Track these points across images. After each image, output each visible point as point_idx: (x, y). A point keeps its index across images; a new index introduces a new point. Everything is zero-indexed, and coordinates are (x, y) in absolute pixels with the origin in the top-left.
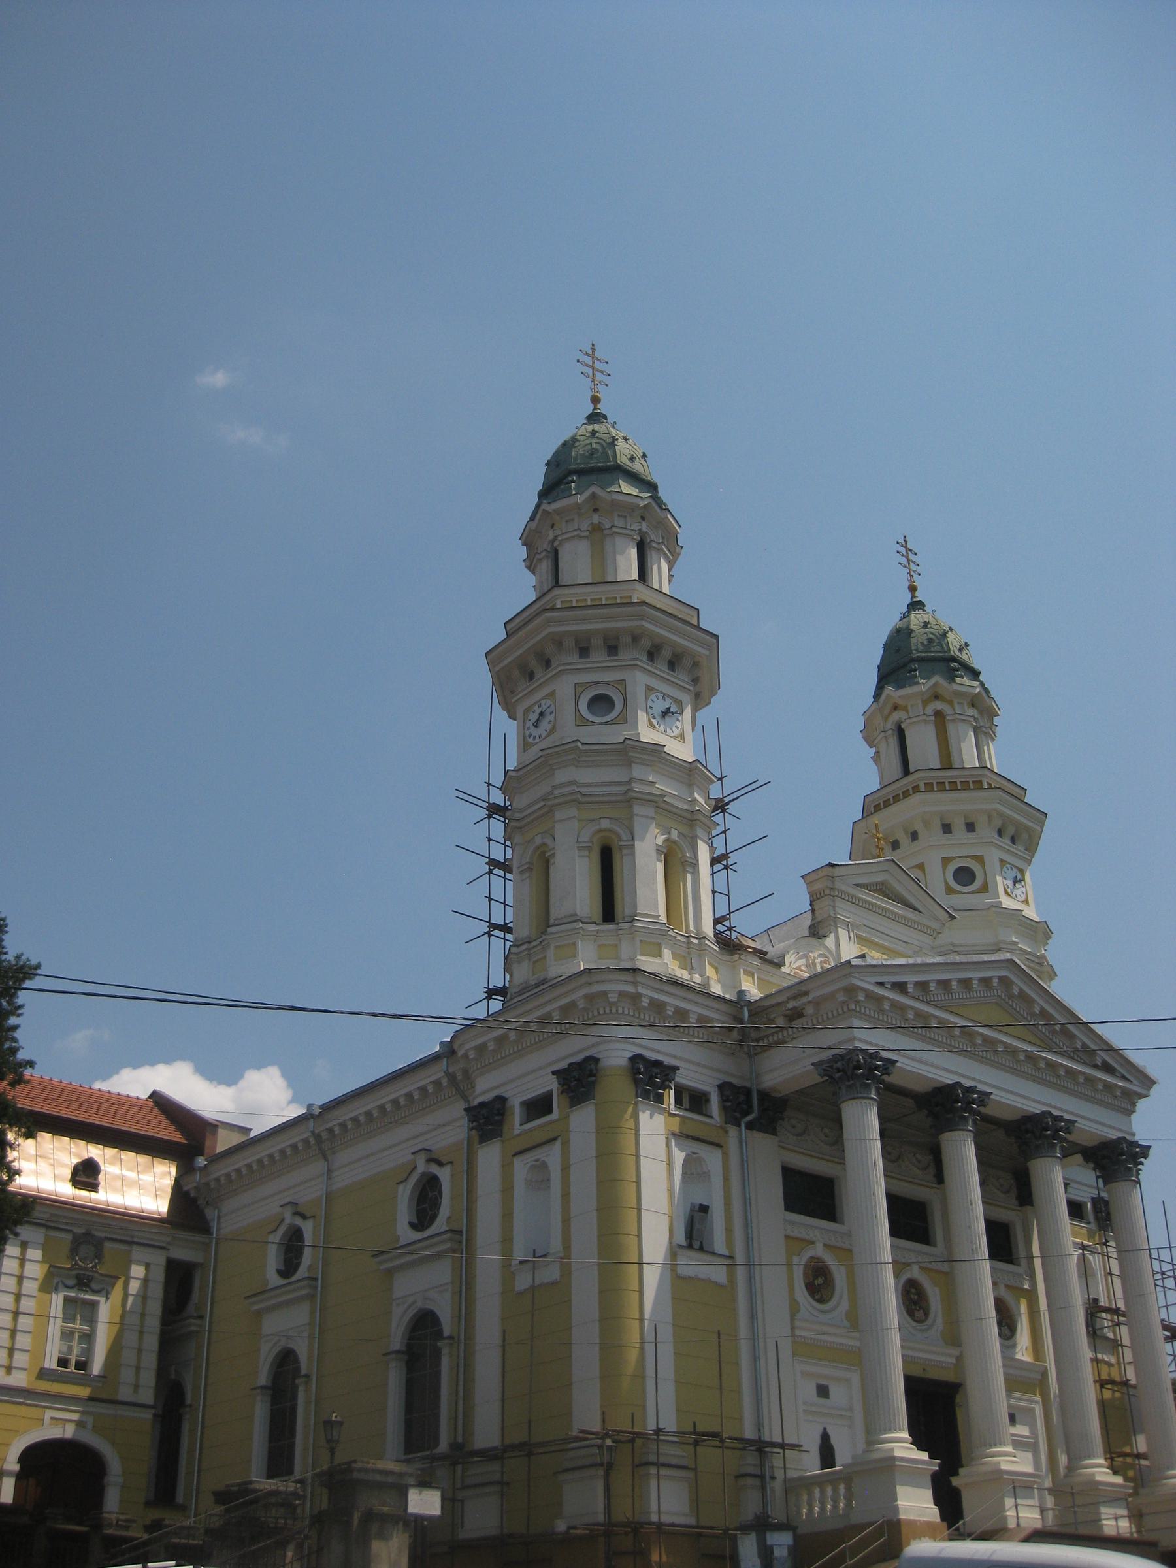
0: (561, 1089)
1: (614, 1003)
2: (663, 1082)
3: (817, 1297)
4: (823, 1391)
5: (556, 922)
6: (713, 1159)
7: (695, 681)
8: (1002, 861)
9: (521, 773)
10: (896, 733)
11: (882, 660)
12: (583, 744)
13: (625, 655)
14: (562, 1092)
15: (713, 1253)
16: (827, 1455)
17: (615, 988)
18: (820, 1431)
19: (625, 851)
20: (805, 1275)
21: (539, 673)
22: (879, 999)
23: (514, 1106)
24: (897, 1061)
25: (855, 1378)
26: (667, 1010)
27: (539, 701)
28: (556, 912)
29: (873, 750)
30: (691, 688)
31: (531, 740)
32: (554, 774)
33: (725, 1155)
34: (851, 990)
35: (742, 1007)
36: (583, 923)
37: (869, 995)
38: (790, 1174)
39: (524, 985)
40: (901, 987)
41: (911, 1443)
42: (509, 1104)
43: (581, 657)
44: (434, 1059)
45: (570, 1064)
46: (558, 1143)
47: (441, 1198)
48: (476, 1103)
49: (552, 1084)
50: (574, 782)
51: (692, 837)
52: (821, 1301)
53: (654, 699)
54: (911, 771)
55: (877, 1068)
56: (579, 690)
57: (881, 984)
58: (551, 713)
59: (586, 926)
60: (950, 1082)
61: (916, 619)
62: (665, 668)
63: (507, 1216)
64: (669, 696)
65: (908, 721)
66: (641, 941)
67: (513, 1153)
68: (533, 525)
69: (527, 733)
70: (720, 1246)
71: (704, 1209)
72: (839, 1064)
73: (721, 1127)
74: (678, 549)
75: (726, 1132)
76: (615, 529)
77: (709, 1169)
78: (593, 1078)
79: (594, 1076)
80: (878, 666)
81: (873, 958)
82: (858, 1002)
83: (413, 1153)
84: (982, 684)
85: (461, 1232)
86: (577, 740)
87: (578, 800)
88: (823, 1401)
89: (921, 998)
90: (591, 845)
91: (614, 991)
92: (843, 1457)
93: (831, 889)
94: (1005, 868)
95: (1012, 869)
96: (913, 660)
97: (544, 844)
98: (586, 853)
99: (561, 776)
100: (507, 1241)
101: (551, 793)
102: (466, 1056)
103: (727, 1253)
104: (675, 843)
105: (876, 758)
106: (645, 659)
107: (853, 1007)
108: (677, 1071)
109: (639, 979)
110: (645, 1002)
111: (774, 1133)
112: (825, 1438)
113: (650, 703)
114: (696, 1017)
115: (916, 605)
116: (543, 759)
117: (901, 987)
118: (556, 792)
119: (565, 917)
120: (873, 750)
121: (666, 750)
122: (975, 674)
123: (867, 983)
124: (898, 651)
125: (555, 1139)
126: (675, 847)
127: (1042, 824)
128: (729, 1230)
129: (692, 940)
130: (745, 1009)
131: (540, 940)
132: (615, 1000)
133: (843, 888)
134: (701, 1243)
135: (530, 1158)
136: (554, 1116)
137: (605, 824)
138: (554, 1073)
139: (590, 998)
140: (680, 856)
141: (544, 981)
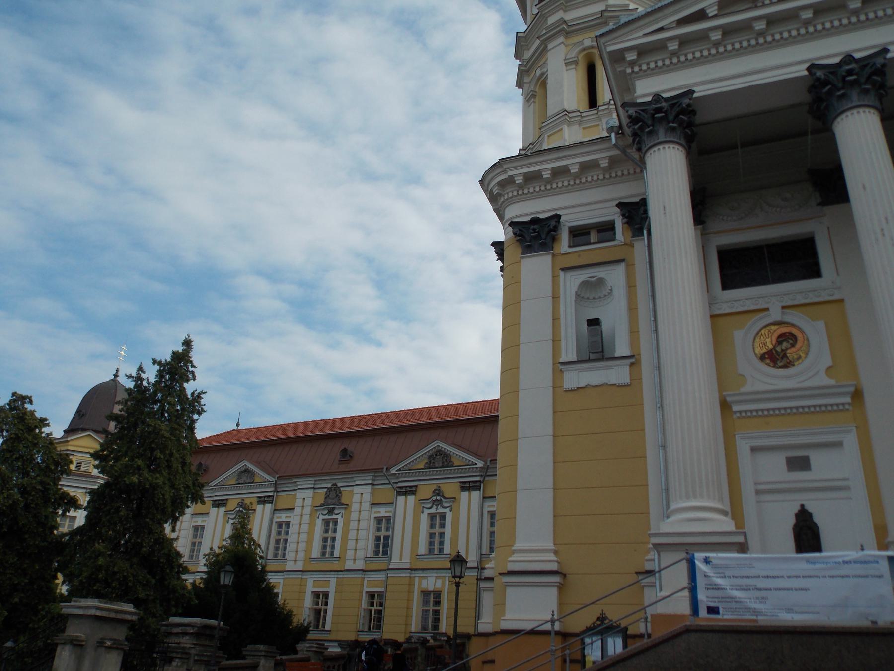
18: (796, 509)
22: (660, 46)
25: (851, 440)
33: (627, 266)
34: (618, 57)
37: (643, 51)
57: (661, 29)
66: (549, 136)
70: (622, 349)
71: (594, 323)
73: (625, 244)
75: (632, 246)
82: (632, 63)
103: (627, 353)
128: (634, 332)
137: (538, 72)
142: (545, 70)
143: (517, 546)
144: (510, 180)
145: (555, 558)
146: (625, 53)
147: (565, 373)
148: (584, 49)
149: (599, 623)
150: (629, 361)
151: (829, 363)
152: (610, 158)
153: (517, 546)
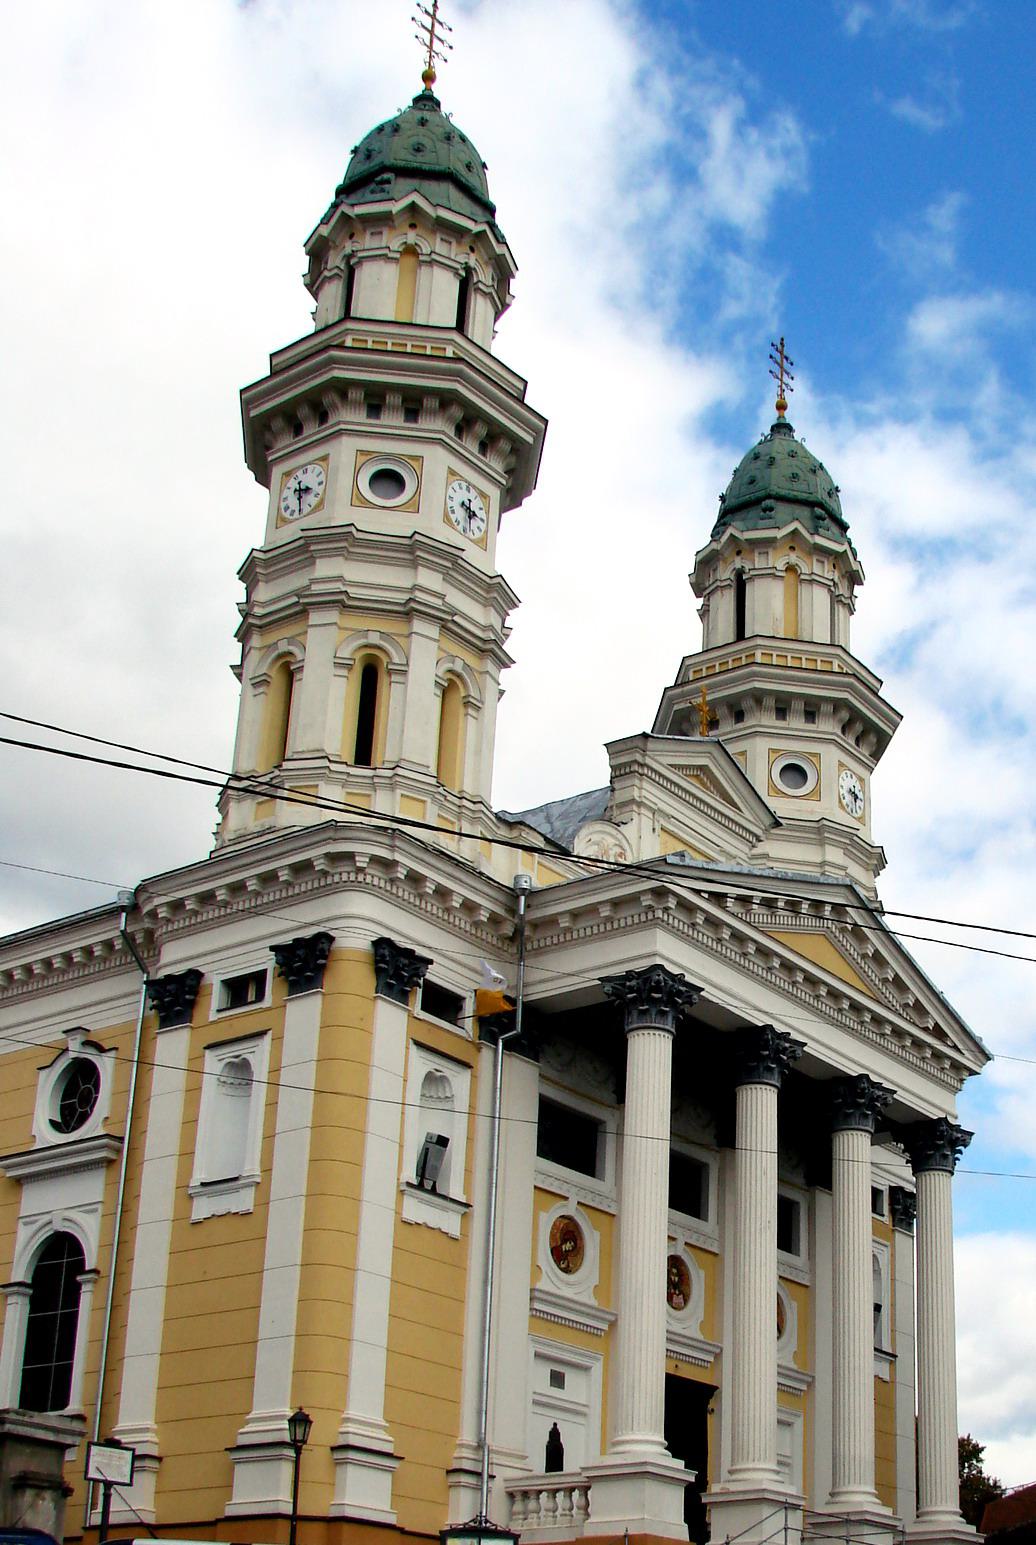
0: (279, 971)
1: (360, 870)
2: (410, 977)
3: (563, 1266)
4: (557, 1380)
5: (295, 757)
6: (459, 1081)
7: (509, 472)
8: (841, 764)
9: (270, 555)
10: (734, 584)
11: (731, 488)
12: (358, 530)
14: (279, 976)
15: (445, 1197)
16: (555, 1456)
17: (364, 850)
19: (394, 678)
20: (553, 1235)
21: (311, 431)
23: (212, 985)
24: (703, 989)
25: (597, 1369)
26: (426, 886)
27: (306, 465)
28: (301, 740)
29: (701, 601)
30: (504, 482)
31: (287, 515)
32: (314, 563)
33: (474, 1077)
34: (660, 893)
35: (518, 897)
36: (330, 761)
38: (548, 1111)
39: (242, 832)
40: (718, 898)
41: (666, 1449)
42: (206, 981)
44: (110, 913)
45: (294, 940)
46: (268, 1038)
47: (97, 1092)
48: (161, 974)
49: (268, 962)
50: (340, 579)
51: (481, 673)
52: (567, 1270)
53: (457, 488)
54: (748, 634)
55: (679, 994)
56: (364, 458)
57: (698, 892)
58: (320, 483)
59: (334, 767)
60: (761, 1024)
61: (780, 446)
62: (475, 449)
63: (190, 1123)
64: (474, 487)
65: (752, 573)
66: (402, 795)
67: (205, 1045)
69: (283, 505)
71: (443, 1141)
72: (634, 983)
75: (479, 1050)
77: (454, 1093)
78: (323, 961)
79: (326, 957)
80: (723, 498)
81: (692, 858)
82: (666, 909)
83: (64, 1032)
84: (850, 544)
85: (121, 1139)
87: (342, 603)
88: (555, 1392)
89: (740, 915)
90: (351, 662)
91: (362, 854)
92: (572, 1462)
93: (642, 765)
94: (843, 775)
95: (852, 777)
96: (769, 497)
97: (290, 654)
98: (344, 672)
99: (325, 568)
100: (187, 1154)
101: (308, 587)
102: (153, 914)
104: (459, 676)
105: (704, 613)
107: (659, 914)
108: (430, 966)
109: (398, 843)
110: (401, 873)
111: (538, 1061)
112: (555, 1434)
113: (450, 492)
114: (461, 901)
115: (782, 428)
116: (302, 542)
117: (718, 898)
118: (313, 587)
119: (309, 751)
120: (701, 601)
121: (463, 555)
122: (844, 527)
123: (682, 888)
124: (752, 481)
125: (262, 1034)
126: (454, 678)
127: (896, 726)
128: (469, 1171)
129: (465, 802)
130: (523, 898)
131: (271, 776)
132: (365, 865)
133: (655, 766)
134: (435, 1183)
135: (228, 1053)
136: (268, 1002)
137: (374, 639)
138: (272, 948)
139: (334, 858)
140: (463, 695)
141: (271, 830)
143: (352, 1413)
144: (388, 865)
145: (390, 1438)
146: (671, 896)
147: (405, 1197)
149: (472, 1524)
150: (463, 1210)
151: (597, 1283)
152: (493, 913)
153: (352, 1413)
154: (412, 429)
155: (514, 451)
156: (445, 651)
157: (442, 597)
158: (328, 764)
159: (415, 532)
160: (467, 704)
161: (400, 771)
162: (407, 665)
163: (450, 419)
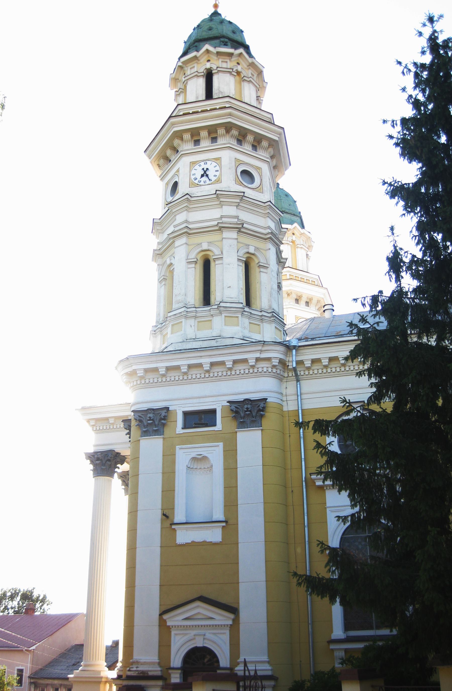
7: (272, 157)
13: (221, 141)
19: (217, 262)
30: (268, 160)
43: (195, 145)
62: (250, 148)
66: (225, 316)
68: (173, 76)
74: (265, 84)
76: (219, 69)
86: (187, 194)
90: (195, 260)
99: (180, 218)
106: (235, 142)
140: (257, 262)
142: (217, 251)
148: (248, 253)
154: (214, 146)
155: (270, 145)
156: (242, 243)
157: (237, 217)
158: (186, 310)
159: (216, 190)
160: (260, 266)
161: (222, 304)
162: (222, 253)
163: (232, 136)
